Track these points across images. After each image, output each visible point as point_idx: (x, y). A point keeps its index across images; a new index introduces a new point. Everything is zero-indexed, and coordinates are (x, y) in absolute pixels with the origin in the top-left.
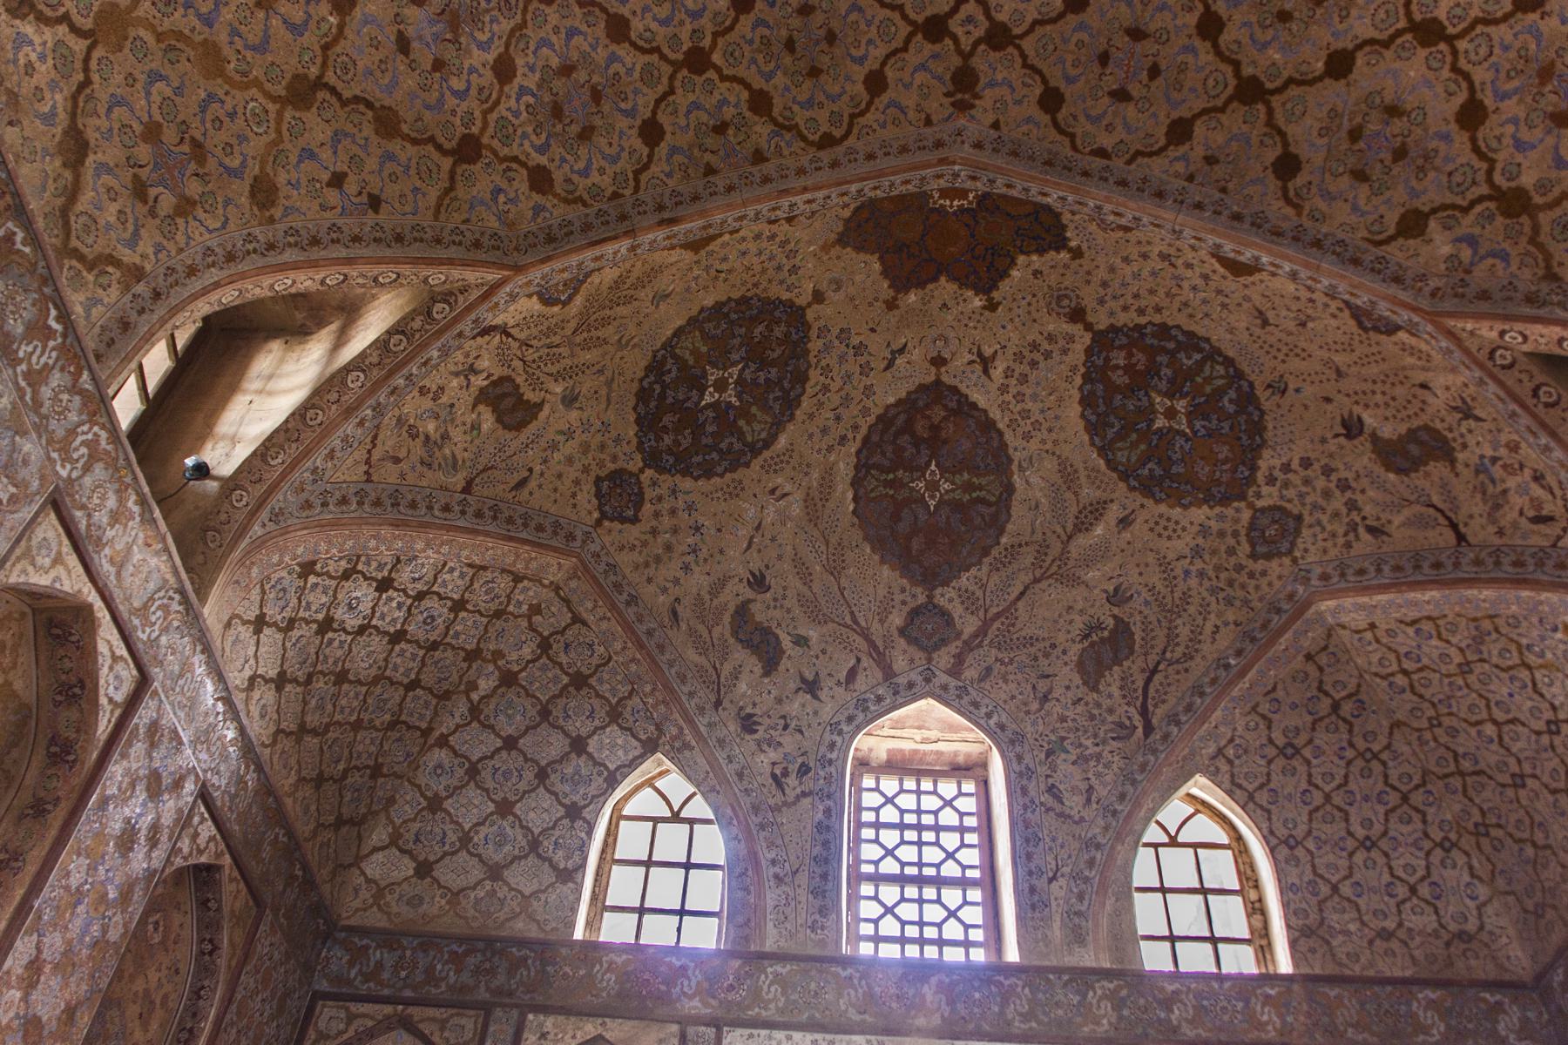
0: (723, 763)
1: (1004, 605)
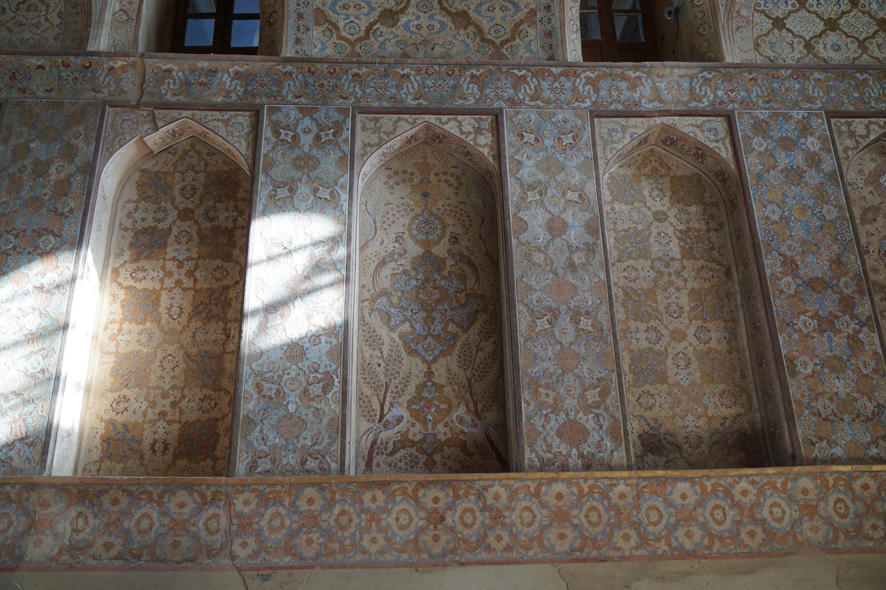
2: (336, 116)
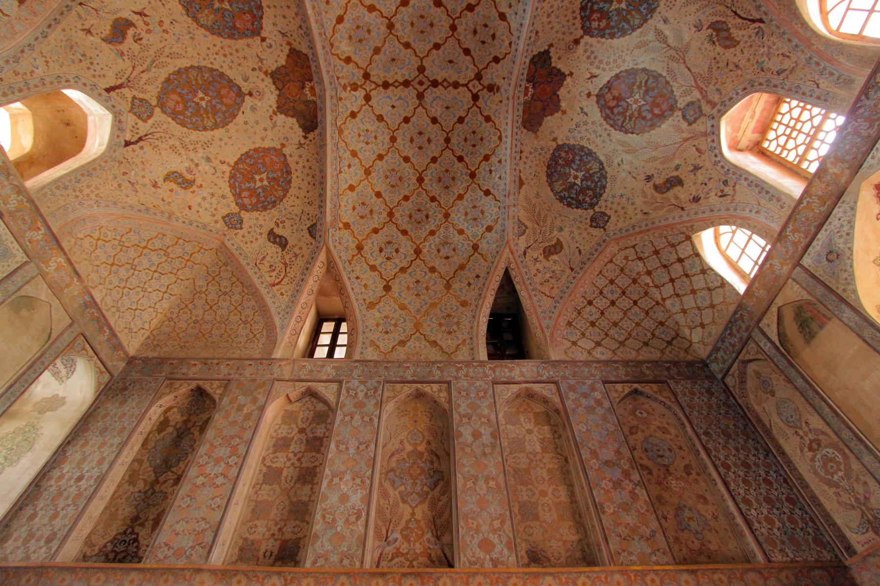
1: (692, 78)
2: (376, 384)
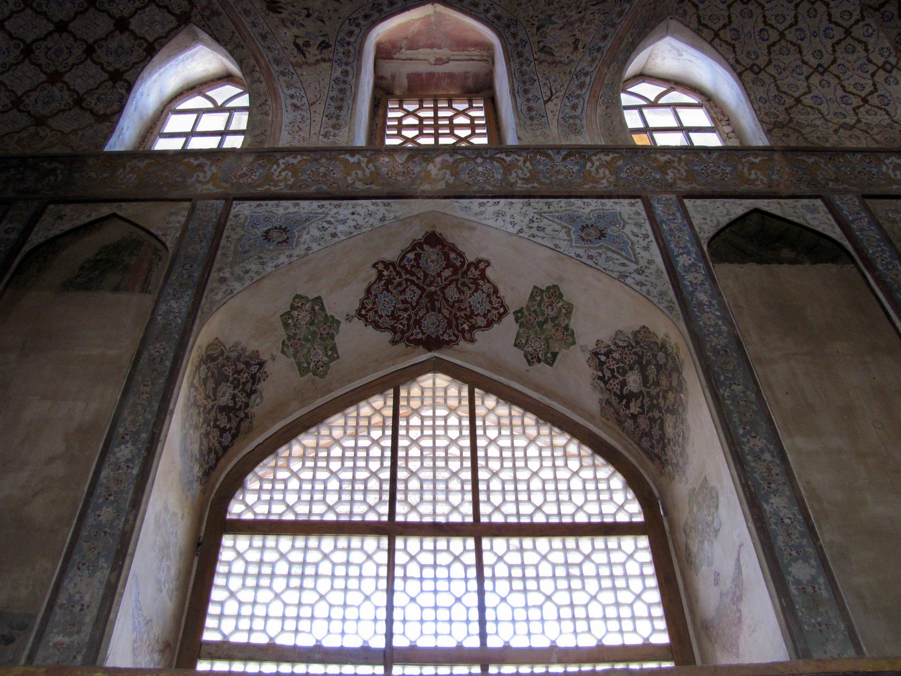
0: (249, 27)
